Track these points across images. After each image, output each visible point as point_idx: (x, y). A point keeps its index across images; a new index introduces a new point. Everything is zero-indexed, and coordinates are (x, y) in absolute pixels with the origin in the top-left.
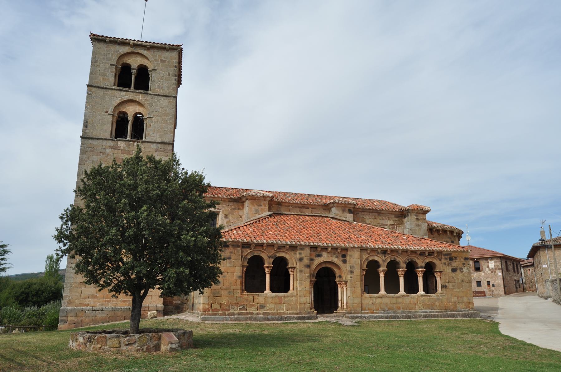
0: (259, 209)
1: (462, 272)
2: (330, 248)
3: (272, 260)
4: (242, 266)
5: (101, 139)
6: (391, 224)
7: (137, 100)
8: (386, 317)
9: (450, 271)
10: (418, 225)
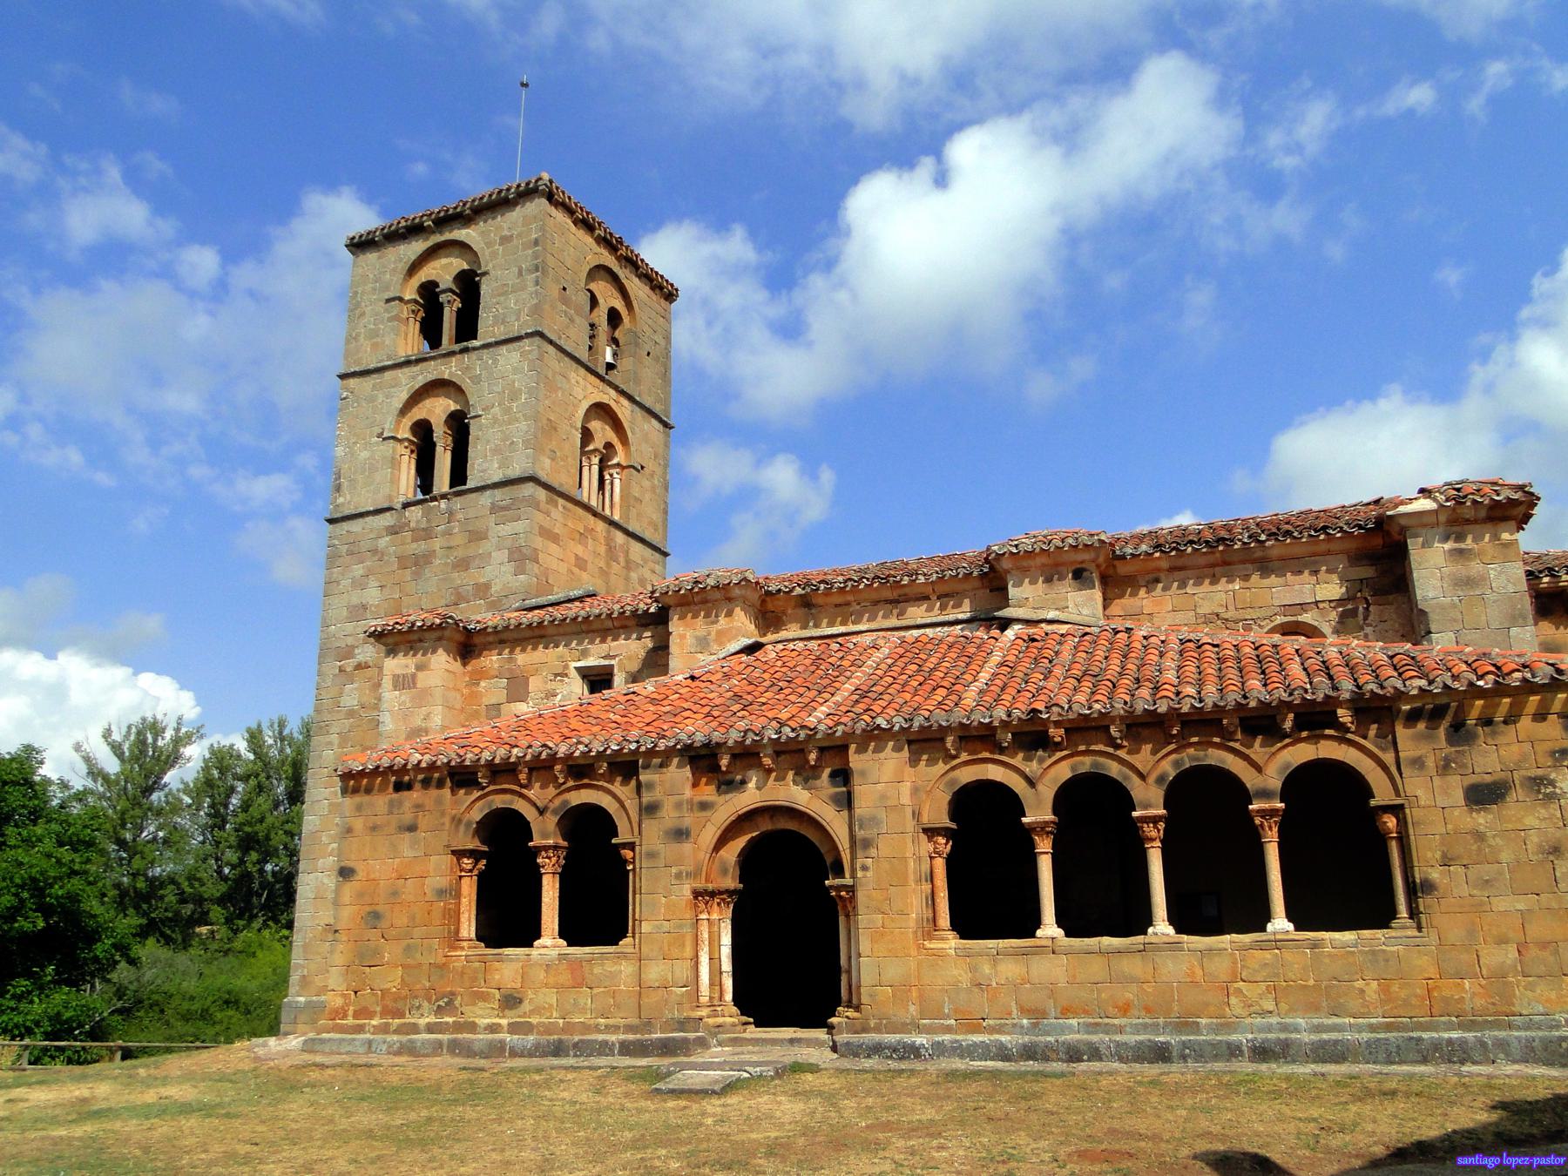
0: (709, 634)
1: (1551, 797)
2: (769, 751)
3: (551, 821)
4: (454, 852)
5: (368, 513)
6: (1330, 601)
7: (446, 377)
8: (1029, 1053)
9: (1459, 796)
10: (1468, 582)
